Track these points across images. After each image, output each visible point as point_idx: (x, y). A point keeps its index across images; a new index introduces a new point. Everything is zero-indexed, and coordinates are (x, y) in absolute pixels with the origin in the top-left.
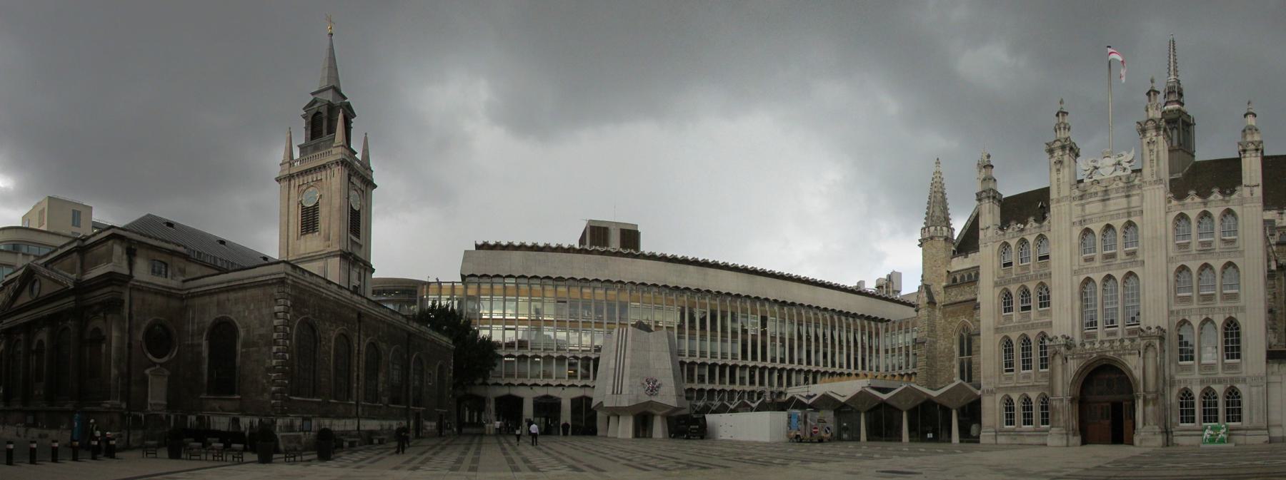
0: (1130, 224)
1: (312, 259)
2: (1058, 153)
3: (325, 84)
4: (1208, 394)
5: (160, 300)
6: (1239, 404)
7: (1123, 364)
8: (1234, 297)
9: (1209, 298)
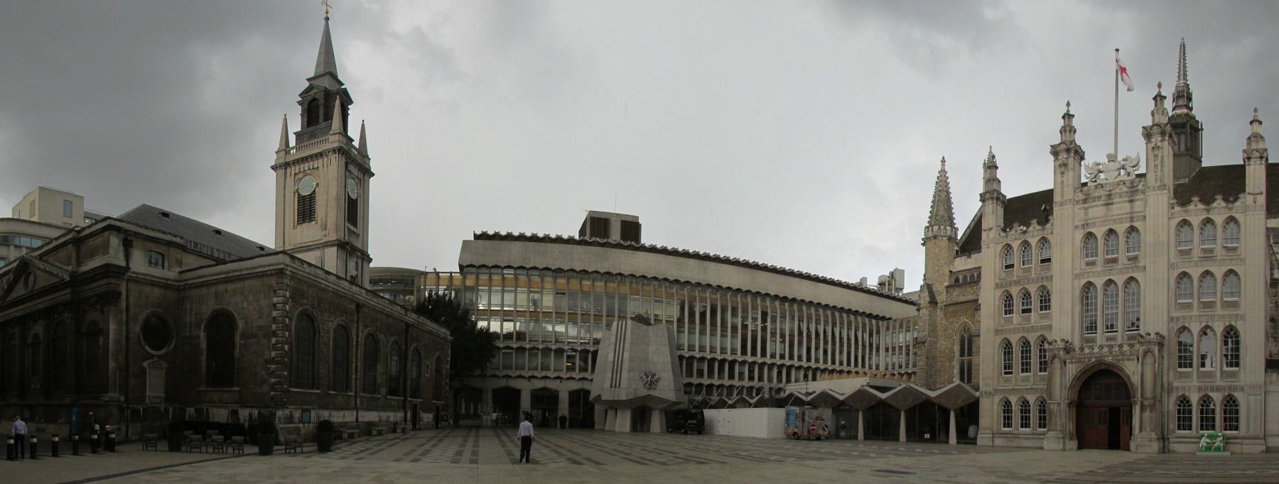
0: (1133, 229)
1: (309, 248)
2: (1063, 156)
3: (321, 71)
4: (1206, 401)
5: (157, 291)
6: (1237, 412)
7: (1123, 370)
8: (1235, 305)
9: (1210, 305)
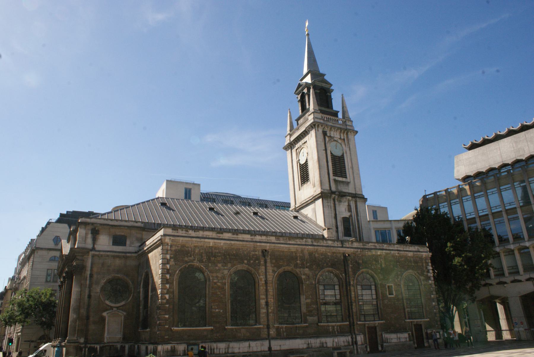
5: (118, 262)
